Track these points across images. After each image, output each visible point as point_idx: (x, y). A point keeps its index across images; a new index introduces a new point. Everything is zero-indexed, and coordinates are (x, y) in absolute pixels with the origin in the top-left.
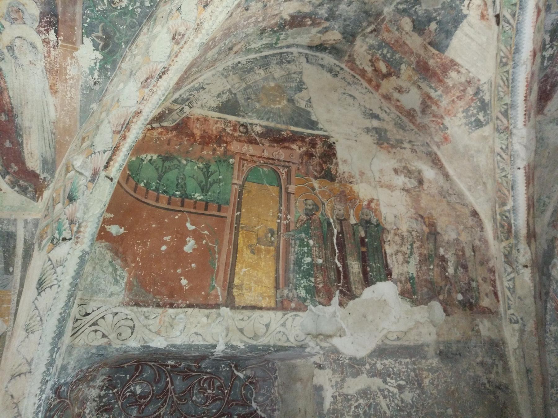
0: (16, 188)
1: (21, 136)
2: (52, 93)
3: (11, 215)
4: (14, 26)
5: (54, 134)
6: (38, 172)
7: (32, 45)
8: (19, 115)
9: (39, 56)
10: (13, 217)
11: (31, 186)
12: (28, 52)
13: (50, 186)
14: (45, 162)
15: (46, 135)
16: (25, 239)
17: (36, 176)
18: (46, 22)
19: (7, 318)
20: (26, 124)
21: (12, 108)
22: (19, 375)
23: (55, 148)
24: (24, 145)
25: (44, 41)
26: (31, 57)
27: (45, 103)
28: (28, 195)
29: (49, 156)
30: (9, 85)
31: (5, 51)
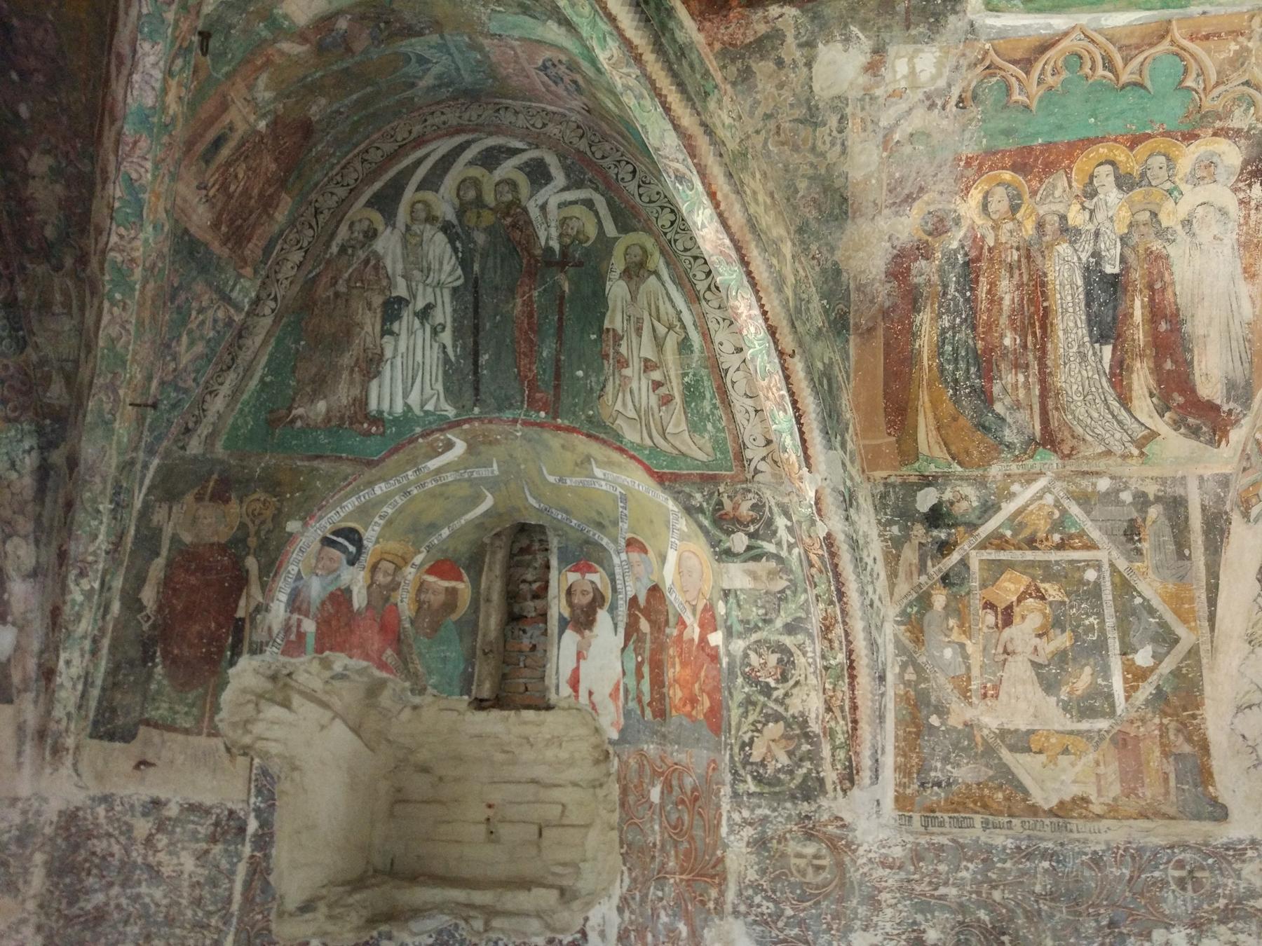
0: (1182, 430)
1: (1191, 351)
2: (1246, 279)
4: (1198, 188)
5: (1249, 341)
6: (1218, 402)
7: (1223, 212)
8: (1189, 319)
9: (1230, 226)
10: (1180, 474)
12: (1213, 222)
13: (1243, 422)
14: (1231, 386)
15: (1234, 344)
17: (1217, 408)
18: (1250, 173)
19: (1193, 624)
20: (1201, 331)
21: (1178, 310)
22: (1250, 707)
23: (1251, 363)
24: (1195, 363)
25: (1241, 202)
26: (1215, 230)
27: (1233, 296)
29: (1239, 376)
30: (1177, 278)
31: (1179, 228)
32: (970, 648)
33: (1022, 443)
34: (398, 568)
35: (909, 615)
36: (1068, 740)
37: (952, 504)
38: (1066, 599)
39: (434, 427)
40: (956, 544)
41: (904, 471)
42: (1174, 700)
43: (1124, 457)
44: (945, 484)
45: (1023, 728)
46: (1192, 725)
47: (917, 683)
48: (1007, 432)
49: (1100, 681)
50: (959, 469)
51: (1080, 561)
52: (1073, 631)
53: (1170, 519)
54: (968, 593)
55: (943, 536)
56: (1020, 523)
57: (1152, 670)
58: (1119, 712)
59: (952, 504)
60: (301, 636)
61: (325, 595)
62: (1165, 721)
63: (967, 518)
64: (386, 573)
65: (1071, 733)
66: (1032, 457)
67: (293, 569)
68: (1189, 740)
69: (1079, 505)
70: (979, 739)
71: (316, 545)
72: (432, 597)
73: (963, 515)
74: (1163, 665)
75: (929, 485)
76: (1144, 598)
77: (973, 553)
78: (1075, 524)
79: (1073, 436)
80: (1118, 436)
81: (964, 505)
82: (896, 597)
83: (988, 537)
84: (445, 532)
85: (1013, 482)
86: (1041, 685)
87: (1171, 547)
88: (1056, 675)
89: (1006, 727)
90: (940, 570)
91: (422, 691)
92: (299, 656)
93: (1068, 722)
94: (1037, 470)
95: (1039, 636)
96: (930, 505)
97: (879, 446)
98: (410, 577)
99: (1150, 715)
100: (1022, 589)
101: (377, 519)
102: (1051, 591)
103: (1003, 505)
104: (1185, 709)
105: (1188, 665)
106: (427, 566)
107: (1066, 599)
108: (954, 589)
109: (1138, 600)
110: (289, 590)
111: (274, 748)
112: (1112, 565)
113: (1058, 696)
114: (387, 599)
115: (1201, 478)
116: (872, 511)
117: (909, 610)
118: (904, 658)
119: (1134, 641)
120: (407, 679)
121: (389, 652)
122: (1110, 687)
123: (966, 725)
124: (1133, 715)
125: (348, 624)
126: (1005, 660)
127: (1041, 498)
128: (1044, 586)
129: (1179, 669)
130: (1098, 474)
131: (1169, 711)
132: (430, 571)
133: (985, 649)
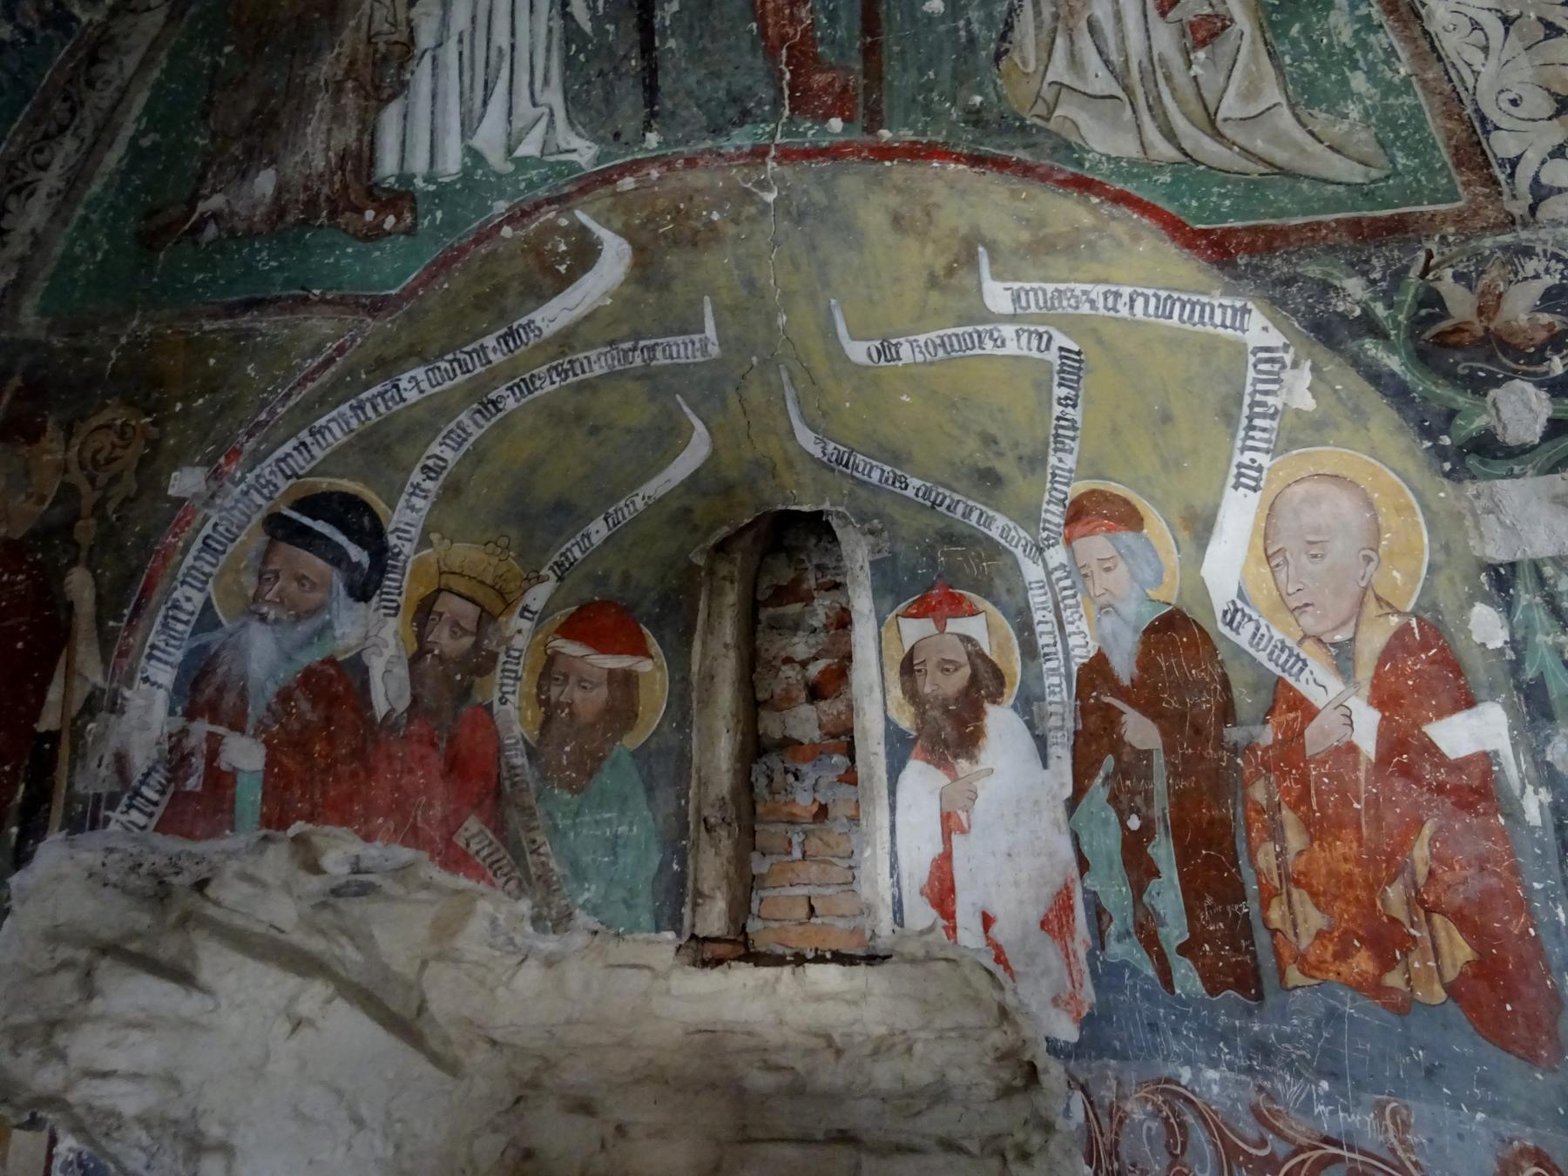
34: (487, 618)
39: (542, 193)
60: (220, 782)
61: (288, 674)
64: (457, 628)
67: (191, 599)
71: (253, 539)
72: (578, 695)
84: (599, 530)
91: (562, 922)
92: (214, 833)
98: (520, 642)
101: (416, 476)
106: (559, 617)
110: (178, 656)
111: (128, 1100)
114: (465, 693)
120: (521, 892)
121: (473, 825)
125: (359, 754)
132: (569, 630)
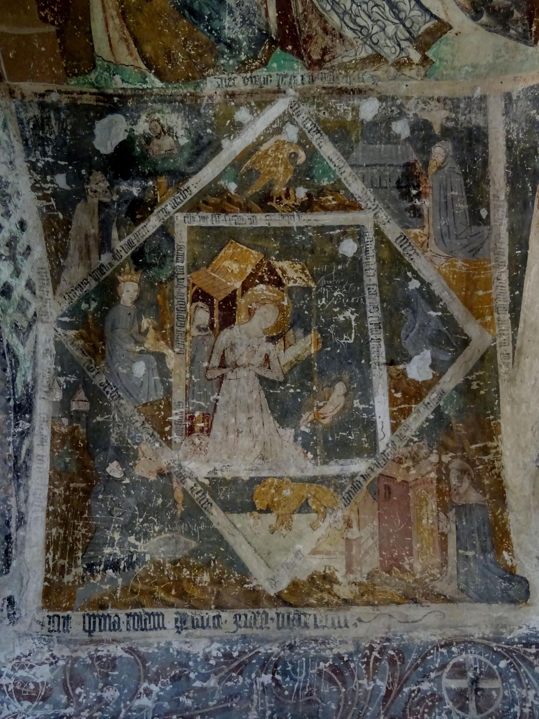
3: (474, 88)
10: (478, 93)
11: (518, 8)
16: (508, 140)
19: (489, 318)
28: (512, 32)
32: (172, 361)
33: (250, 40)
35: (85, 315)
36: (308, 491)
37: (149, 140)
38: (313, 285)
40: (154, 203)
41: (73, 85)
42: (459, 427)
43: (399, 65)
44: (138, 110)
45: (245, 476)
46: (482, 462)
47: (91, 415)
48: (227, 21)
49: (356, 403)
50: (158, 84)
51: (333, 228)
52: (320, 331)
53: (462, 163)
54: (171, 278)
55: (135, 191)
56: (250, 171)
57: (429, 385)
58: (382, 447)
59: (149, 140)
62: (446, 459)
63: (170, 164)
65: (313, 480)
66: (264, 64)
68: (477, 485)
69: (334, 142)
70: (179, 495)
73: (164, 159)
74: (446, 378)
75: (114, 110)
76: (422, 281)
77: (180, 217)
78: (327, 171)
79: (325, 31)
80: (390, 29)
81: (167, 142)
82: (64, 286)
83: (203, 193)
85: (238, 106)
86: (273, 412)
87: (462, 206)
88: (295, 396)
89: (220, 474)
90: (130, 244)
93: (310, 465)
94: (272, 86)
95: (272, 340)
96: (116, 142)
97: (27, 38)
99: (425, 450)
100: (249, 271)
102: (291, 273)
103: (225, 143)
104: (473, 441)
105: (479, 378)
107: (313, 285)
108: (152, 273)
109: (414, 284)
112: (378, 232)
113: (296, 427)
115: (508, 97)
116: (18, 147)
117: (84, 306)
118: (72, 379)
119: (407, 344)
122: (371, 411)
123: (161, 474)
124: (402, 451)
126: (222, 378)
127: (279, 131)
128: (279, 265)
129: (467, 382)
130: (360, 92)
131: (450, 443)
133: (192, 360)
